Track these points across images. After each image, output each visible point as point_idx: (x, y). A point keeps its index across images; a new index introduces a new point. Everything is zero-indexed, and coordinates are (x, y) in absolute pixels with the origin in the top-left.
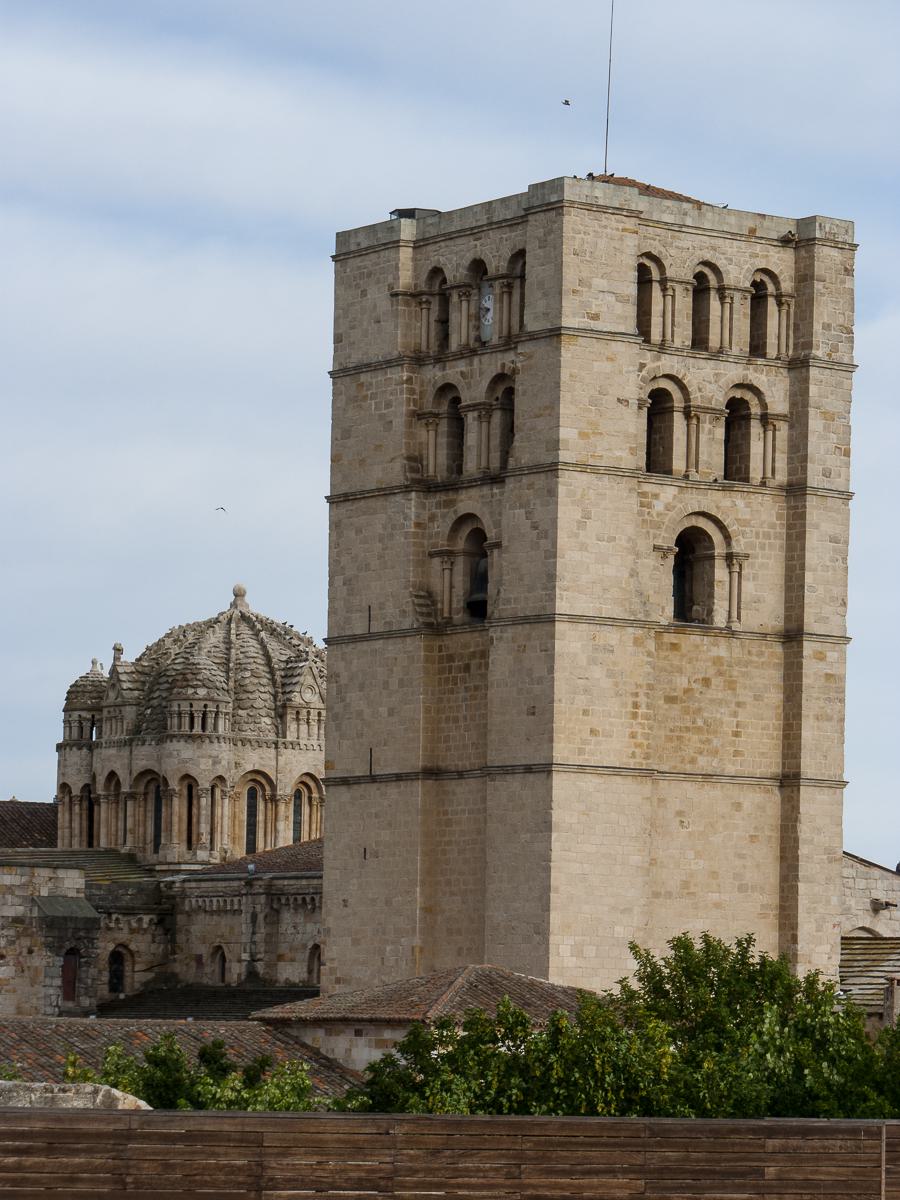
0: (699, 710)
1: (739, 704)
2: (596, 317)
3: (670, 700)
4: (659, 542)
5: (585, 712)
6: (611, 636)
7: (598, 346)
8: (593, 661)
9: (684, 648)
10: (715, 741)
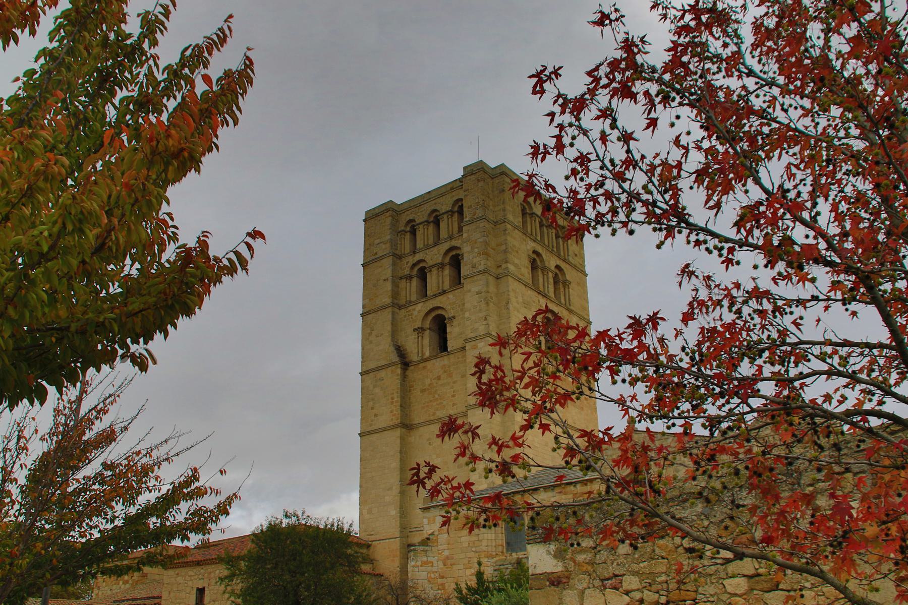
0: (436, 391)
1: (454, 382)
2: (376, 254)
3: (423, 391)
4: (416, 327)
5: (372, 408)
6: (382, 374)
7: (376, 264)
8: (375, 387)
9: (429, 367)
10: (445, 403)
